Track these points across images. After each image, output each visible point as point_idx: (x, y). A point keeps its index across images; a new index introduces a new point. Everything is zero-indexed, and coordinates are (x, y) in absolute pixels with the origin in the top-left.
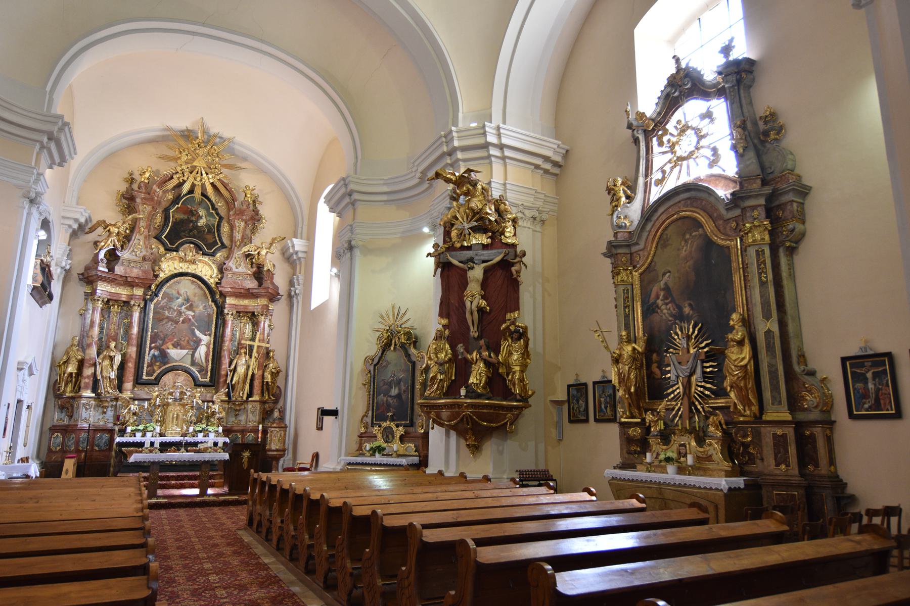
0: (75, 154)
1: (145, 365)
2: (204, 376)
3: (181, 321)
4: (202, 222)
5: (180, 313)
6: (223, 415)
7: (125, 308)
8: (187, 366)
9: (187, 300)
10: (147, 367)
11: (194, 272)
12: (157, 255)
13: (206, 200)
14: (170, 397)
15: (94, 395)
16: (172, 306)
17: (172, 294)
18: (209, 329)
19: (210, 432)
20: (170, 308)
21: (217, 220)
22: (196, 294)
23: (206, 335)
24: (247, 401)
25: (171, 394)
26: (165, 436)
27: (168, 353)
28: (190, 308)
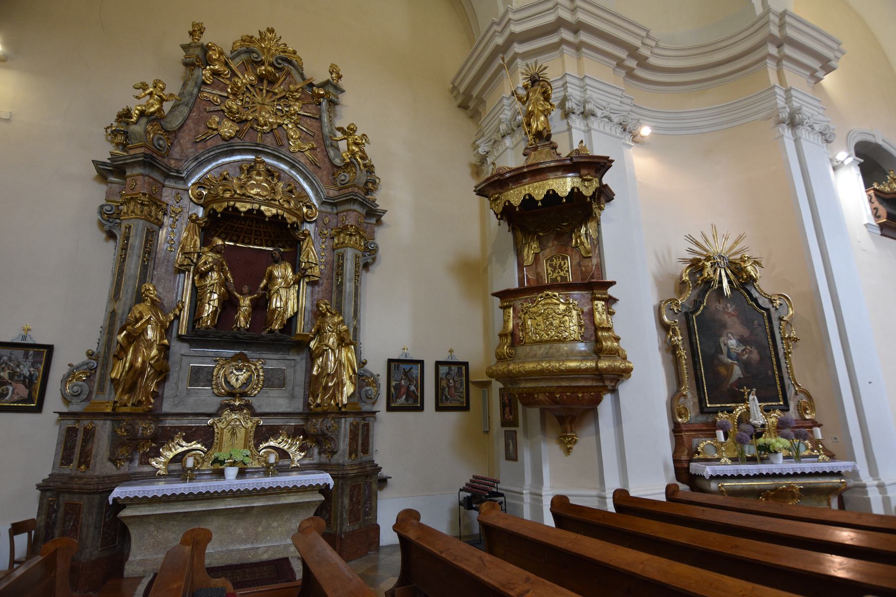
0: (839, 44)
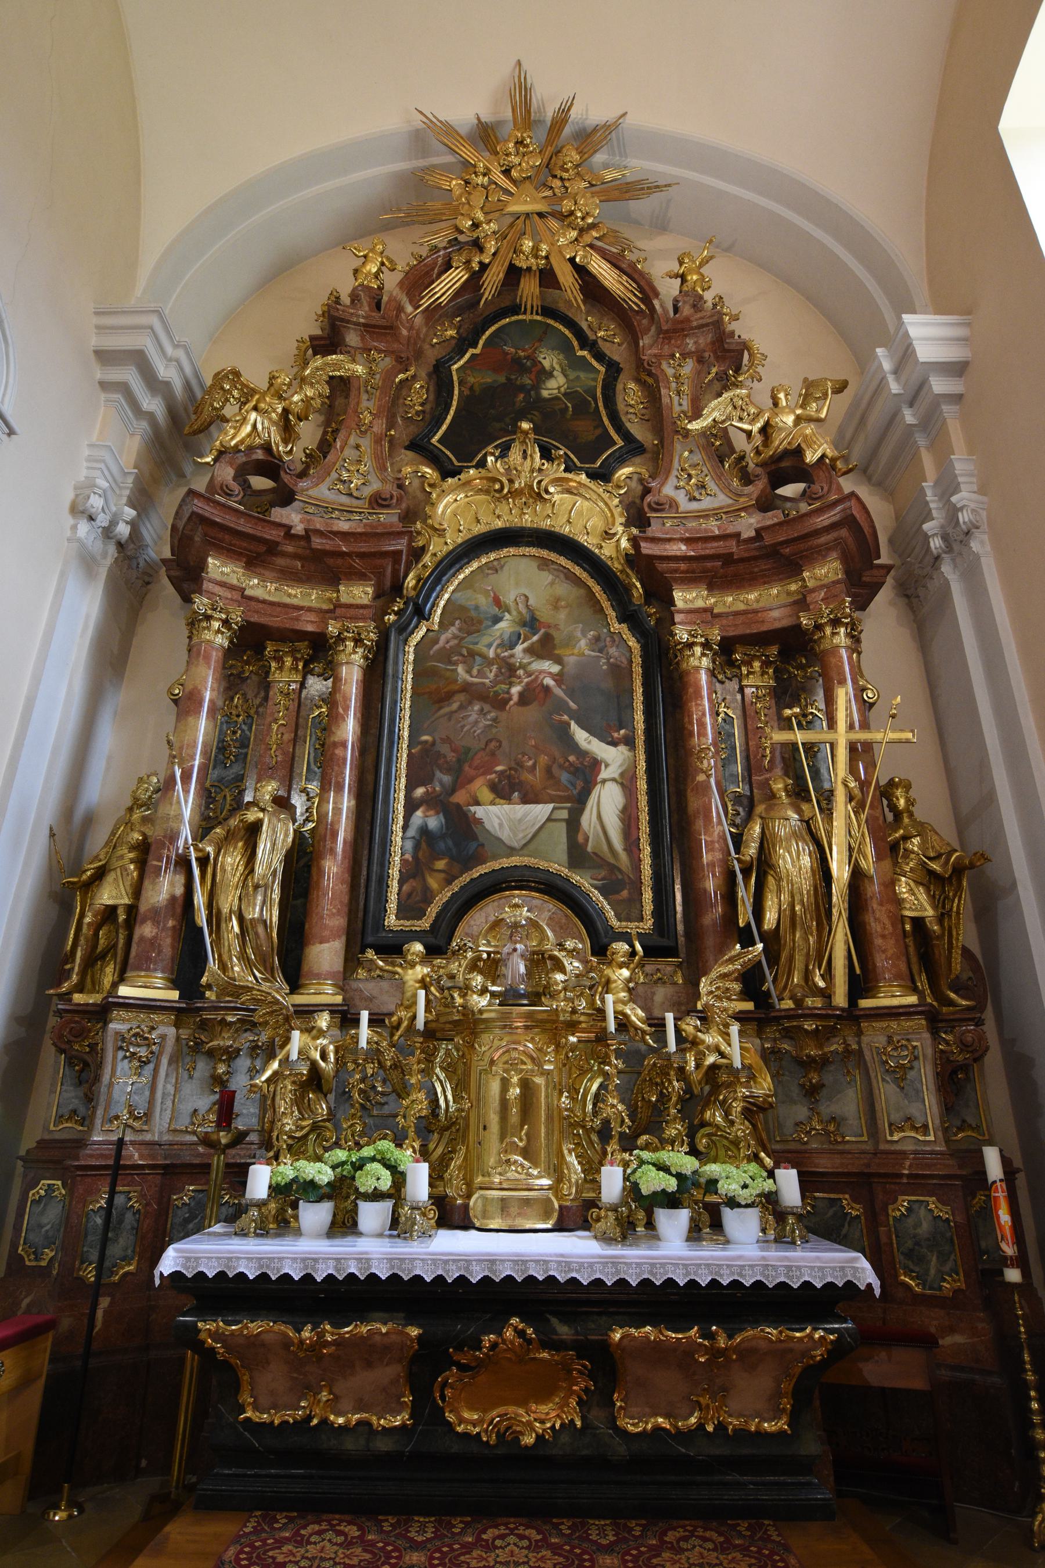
1: (395, 872)
2: (630, 910)
3: (515, 698)
4: (554, 386)
5: (509, 670)
6: (764, 1086)
7: (318, 667)
8: (554, 867)
9: (531, 623)
10: (401, 883)
11: (546, 524)
12: (419, 494)
13: (557, 325)
14: (478, 980)
15: (175, 995)
16: (481, 647)
17: (477, 608)
18: (624, 720)
19: (733, 1203)
20: (472, 654)
21: (601, 377)
22: (558, 600)
23: (614, 743)
24: (853, 1016)
25: (492, 967)
26: (466, 1225)
27: (479, 822)
28: (545, 649)
